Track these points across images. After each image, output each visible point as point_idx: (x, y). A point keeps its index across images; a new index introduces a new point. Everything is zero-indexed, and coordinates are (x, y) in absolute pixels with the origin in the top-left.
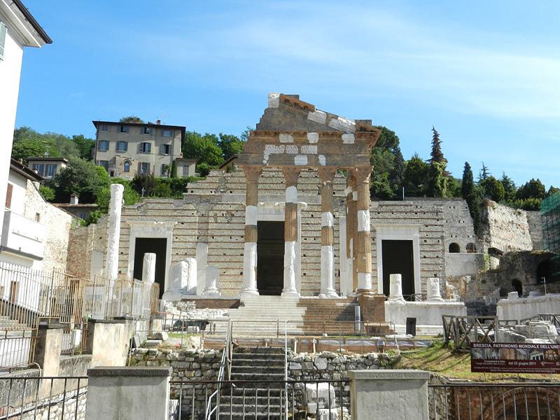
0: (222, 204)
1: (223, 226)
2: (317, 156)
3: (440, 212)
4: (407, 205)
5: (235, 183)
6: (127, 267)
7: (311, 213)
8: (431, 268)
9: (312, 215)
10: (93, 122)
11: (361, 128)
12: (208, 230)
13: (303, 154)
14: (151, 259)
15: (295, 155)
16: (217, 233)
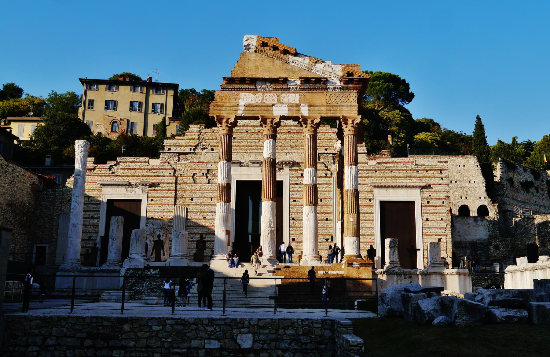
0: (203, 163)
1: (203, 187)
3: (444, 170)
4: (407, 163)
5: (216, 139)
6: (97, 233)
8: (434, 231)
10: (80, 79)
11: (348, 72)
12: (186, 191)
13: (283, 103)
14: (117, 223)
15: (273, 105)
16: (197, 194)
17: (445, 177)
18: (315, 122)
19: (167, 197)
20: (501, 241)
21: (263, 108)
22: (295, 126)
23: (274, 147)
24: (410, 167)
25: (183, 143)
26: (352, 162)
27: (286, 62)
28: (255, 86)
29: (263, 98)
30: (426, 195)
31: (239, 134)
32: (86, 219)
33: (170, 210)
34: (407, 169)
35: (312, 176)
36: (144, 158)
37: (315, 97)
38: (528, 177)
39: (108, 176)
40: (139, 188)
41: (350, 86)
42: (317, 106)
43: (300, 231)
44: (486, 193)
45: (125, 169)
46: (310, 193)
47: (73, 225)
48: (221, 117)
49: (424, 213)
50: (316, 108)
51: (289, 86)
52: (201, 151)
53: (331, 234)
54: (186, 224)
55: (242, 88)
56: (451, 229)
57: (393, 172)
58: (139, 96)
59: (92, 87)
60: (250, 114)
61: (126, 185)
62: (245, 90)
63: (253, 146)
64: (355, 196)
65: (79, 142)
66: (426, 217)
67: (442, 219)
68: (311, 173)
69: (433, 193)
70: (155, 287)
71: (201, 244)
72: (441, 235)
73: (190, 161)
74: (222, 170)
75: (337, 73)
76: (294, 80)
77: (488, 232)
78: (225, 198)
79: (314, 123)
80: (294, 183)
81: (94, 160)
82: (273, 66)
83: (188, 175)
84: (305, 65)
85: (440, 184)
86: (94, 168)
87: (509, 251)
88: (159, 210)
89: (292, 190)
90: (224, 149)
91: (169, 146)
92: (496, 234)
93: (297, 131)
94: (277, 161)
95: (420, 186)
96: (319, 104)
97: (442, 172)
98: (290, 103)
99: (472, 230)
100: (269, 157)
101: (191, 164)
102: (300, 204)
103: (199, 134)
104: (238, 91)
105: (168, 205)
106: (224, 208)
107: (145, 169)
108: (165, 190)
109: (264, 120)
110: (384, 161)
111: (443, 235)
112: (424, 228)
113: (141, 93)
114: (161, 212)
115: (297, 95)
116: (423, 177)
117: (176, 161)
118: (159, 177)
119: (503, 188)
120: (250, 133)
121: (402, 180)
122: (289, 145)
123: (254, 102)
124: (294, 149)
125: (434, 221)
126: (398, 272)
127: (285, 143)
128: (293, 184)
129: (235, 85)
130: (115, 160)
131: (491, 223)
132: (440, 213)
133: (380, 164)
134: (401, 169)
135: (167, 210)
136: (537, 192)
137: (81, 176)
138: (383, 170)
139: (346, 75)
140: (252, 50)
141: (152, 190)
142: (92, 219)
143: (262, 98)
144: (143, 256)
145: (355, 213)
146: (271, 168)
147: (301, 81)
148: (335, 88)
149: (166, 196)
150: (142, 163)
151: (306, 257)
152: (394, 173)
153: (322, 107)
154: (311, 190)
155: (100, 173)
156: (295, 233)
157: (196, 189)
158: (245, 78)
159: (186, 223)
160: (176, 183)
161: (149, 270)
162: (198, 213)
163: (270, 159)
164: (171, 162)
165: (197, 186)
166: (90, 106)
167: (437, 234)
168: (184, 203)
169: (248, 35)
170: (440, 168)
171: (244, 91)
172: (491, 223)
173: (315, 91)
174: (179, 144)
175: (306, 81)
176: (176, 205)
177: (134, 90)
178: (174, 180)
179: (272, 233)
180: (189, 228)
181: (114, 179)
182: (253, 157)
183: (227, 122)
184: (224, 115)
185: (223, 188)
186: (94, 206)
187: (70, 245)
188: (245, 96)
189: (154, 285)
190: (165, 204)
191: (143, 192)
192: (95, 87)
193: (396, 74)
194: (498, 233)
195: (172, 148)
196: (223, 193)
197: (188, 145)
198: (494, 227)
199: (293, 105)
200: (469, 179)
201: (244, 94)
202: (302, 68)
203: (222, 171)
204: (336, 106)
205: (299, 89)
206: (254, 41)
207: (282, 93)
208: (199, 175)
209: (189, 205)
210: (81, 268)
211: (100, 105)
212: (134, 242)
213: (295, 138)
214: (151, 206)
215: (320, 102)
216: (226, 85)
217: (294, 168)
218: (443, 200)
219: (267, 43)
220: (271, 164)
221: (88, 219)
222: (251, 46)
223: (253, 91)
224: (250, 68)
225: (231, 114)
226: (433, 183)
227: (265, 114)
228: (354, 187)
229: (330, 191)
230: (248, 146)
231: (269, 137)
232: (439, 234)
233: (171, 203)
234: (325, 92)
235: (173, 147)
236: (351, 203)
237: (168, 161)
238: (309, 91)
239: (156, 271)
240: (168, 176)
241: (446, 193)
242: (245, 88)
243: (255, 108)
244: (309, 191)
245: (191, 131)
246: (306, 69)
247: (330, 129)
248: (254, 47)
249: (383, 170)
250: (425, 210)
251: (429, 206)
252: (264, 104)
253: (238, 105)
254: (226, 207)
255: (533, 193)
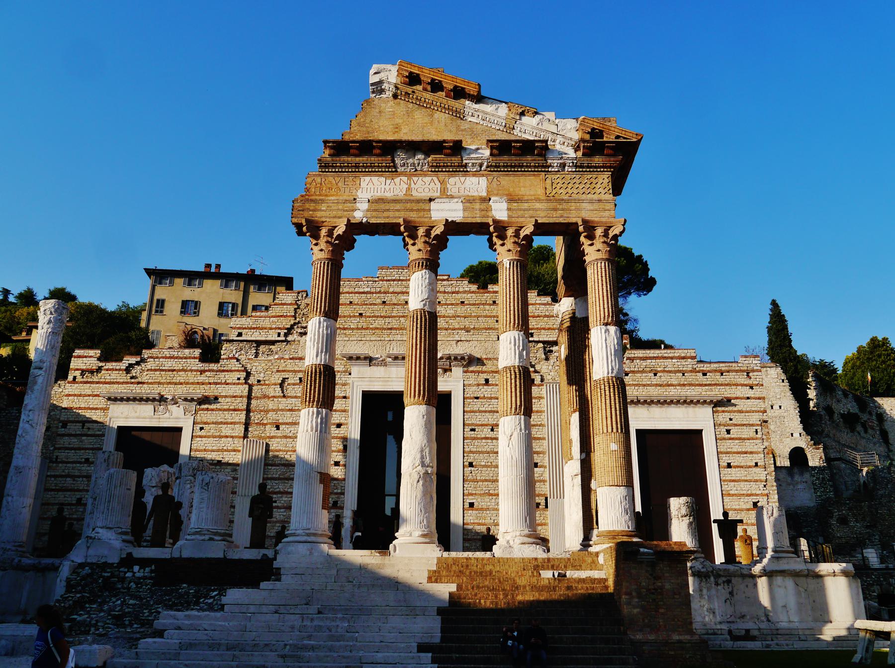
2: (486, 200)
3: (753, 371)
4: (683, 358)
7: (485, 376)
8: (744, 488)
9: (487, 381)
10: (145, 269)
11: (593, 129)
12: (267, 411)
13: (452, 197)
15: (431, 200)
17: (757, 385)
18: (522, 234)
19: (231, 423)
20: (850, 509)
21: (409, 205)
22: (473, 292)
23: (432, 289)
24: (691, 366)
25: (267, 323)
26: (608, 318)
27: (459, 115)
28: (393, 161)
29: (410, 185)
30: (723, 417)
31: (370, 307)
32: (74, 465)
33: (234, 447)
34: (684, 369)
35: (519, 349)
36: (192, 350)
37: (521, 184)
38: (848, 406)
39: (123, 383)
40: (179, 407)
41: (596, 159)
42: (527, 201)
43: (484, 489)
44: (801, 426)
45: (155, 370)
46: (516, 385)
47: (17, 468)
48: (317, 222)
49: (722, 453)
50: (526, 205)
51: (465, 162)
52: (299, 338)
53: (545, 494)
54: (264, 474)
55: (363, 166)
56: (775, 484)
57: (659, 374)
58: (233, 295)
59: (164, 281)
60: (380, 217)
61: (154, 400)
62: (371, 170)
63: (396, 329)
64: (619, 393)
65: (46, 304)
66: (726, 459)
67: (756, 464)
68: (517, 341)
69: (736, 414)
70: (129, 612)
71: (261, 506)
72: (757, 495)
73: (276, 357)
74: (314, 335)
75: (569, 135)
76: (477, 147)
77: (814, 495)
78: (319, 398)
79: (521, 237)
80: (472, 396)
81: (99, 355)
82: (432, 123)
83: (273, 382)
84: (498, 119)
85: (748, 398)
86: (99, 370)
87: (867, 527)
88: (214, 448)
89: (468, 409)
90: (322, 290)
91: (239, 328)
92: (829, 498)
93: (477, 302)
94: (439, 355)
95: (712, 401)
96: (530, 198)
97: (751, 374)
98: (468, 196)
99: (785, 490)
100: (422, 307)
101: (279, 361)
102: (483, 436)
103: (296, 307)
104: (355, 171)
105: (232, 437)
106: (315, 421)
107: (191, 371)
108: (229, 410)
109: (412, 230)
110: (641, 355)
111: (762, 495)
112: (724, 481)
113: (235, 290)
114: (218, 451)
115: (483, 181)
116: (715, 384)
117: (250, 357)
118: (218, 386)
119: (821, 421)
120: (390, 304)
121: (676, 390)
122: (462, 327)
123: (389, 195)
124: (471, 333)
125: (742, 467)
126: (702, 570)
127: (455, 323)
128: (470, 398)
129: (350, 159)
130: (139, 353)
131: (818, 479)
132: (751, 453)
133: (633, 360)
134: (673, 369)
135: (229, 448)
136: (866, 432)
137: (44, 369)
138: (638, 372)
139: (587, 137)
140: (389, 94)
141: (203, 410)
142: (86, 465)
143: (407, 186)
144: (125, 533)
145: (622, 431)
146: (425, 332)
147: (492, 148)
148: (563, 166)
149: (229, 421)
150: (188, 360)
151: (508, 537)
152: (660, 376)
153: (538, 204)
154: (518, 380)
155: (109, 377)
156: (474, 492)
157: (287, 408)
158: (371, 142)
159: (264, 471)
160: (249, 397)
161: (130, 568)
162: (289, 453)
163: (424, 312)
164: (242, 358)
165: (287, 402)
166: (159, 309)
167: (749, 492)
168: (263, 435)
169: (379, 65)
170: (746, 368)
171: (369, 172)
172: (818, 479)
173: (521, 171)
174: (258, 326)
175: (501, 148)
176: (248, 438)
177: (226, 286)
178: (245, 391)
179: (428, 479)
180: (269, 481)
181: (134, 388)
182: (395, 349)
183: (330, 233)
184: (324, 219)
185: (316, 375)
186: (92, 439)
187: (5, 510)
188: (371, 184)
189: (128, 605)
190: (227, 437)
191: (187, 413)
192: (168, 282)
193: (628, 246)
194: (833, 496)
195: (244, 331)
196: (315, 388)
197: (274, 326)
198: (825, 484)
199: (474, 200)
200: (770, 403)
201: (367, 179)
202: (493, 127)
203: (315, 339)
204: (567, 201)
205: (488, 167)
206: (391, 75)
207: (449, 177)
208: (293, 382)
209: (272, 437)
210: (20, 561)
211: (173, 308)
212: (103, 500)
213: (473, 314)
214: (200, 439)
215: (532, 193)
216: (330, 159)
217: (471, 369)
218: (757, 428)
219: (418, 75)
220: (425, 324)
221: (78, 465)
222: (385, 85)
223: (388, 171)
224: (382, 128)
225: (340, 217)
226: (734, 396)
227: (413, 216)
228: (615, 372)
229: (541, 412)
230: (385, 329)
231: (422, 266)
232: (754, 492)
233: (237, 434)
234: (543, 173)
235: (247, 331)
236: (611, 408)
237: (237, 356)
238: (508, 171)
239: (147, 569)
240: (234, 384)
241: (761, 414)
242: (371, 167)
243: (392, 206)
244: (513, 381)
245: (280, 302)
246: (501, 128)
247: (538, 298)
248: (392, 87)
249: (638, 372)
250: (725, 446)
251: (730, 439)
252: (412, 198)
253: (355, 199)
254: (322, 419)
255: (859, 434)
